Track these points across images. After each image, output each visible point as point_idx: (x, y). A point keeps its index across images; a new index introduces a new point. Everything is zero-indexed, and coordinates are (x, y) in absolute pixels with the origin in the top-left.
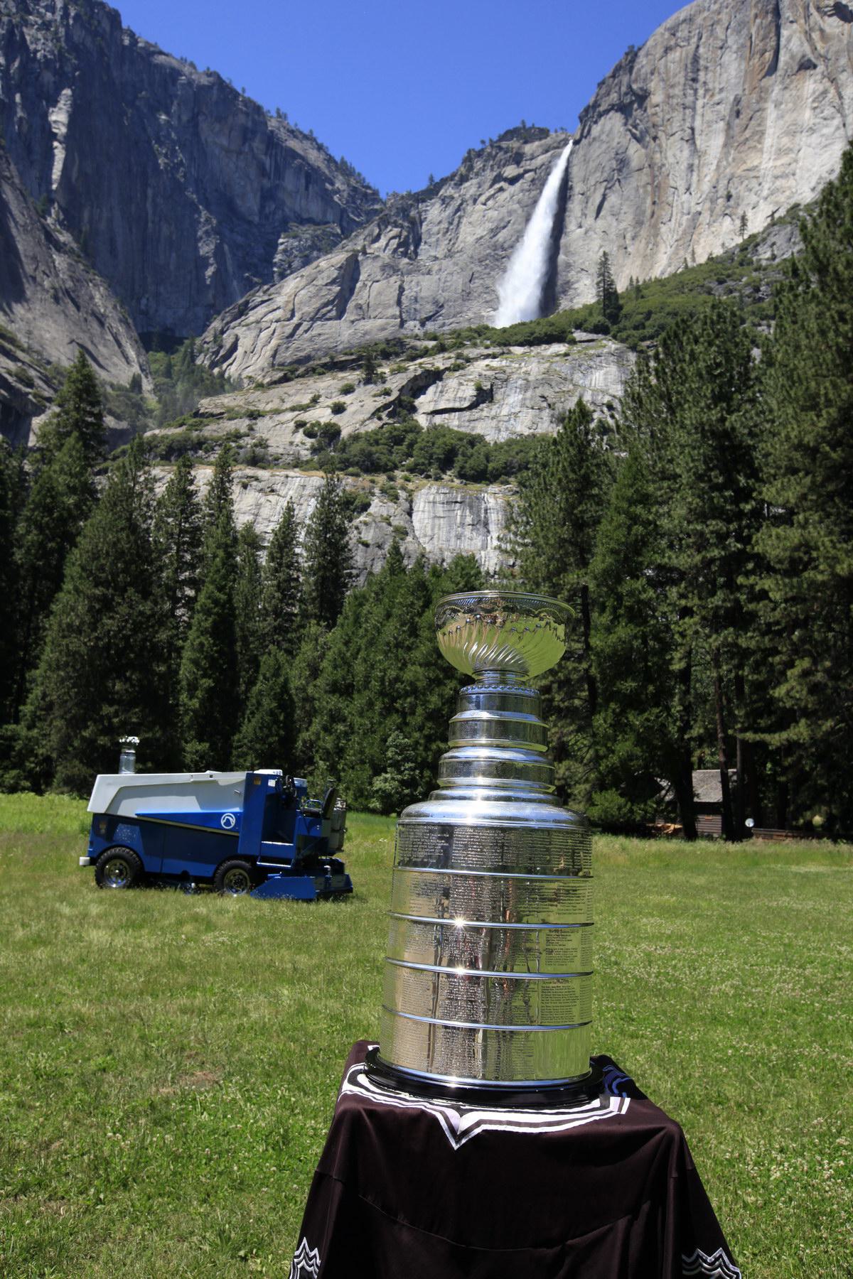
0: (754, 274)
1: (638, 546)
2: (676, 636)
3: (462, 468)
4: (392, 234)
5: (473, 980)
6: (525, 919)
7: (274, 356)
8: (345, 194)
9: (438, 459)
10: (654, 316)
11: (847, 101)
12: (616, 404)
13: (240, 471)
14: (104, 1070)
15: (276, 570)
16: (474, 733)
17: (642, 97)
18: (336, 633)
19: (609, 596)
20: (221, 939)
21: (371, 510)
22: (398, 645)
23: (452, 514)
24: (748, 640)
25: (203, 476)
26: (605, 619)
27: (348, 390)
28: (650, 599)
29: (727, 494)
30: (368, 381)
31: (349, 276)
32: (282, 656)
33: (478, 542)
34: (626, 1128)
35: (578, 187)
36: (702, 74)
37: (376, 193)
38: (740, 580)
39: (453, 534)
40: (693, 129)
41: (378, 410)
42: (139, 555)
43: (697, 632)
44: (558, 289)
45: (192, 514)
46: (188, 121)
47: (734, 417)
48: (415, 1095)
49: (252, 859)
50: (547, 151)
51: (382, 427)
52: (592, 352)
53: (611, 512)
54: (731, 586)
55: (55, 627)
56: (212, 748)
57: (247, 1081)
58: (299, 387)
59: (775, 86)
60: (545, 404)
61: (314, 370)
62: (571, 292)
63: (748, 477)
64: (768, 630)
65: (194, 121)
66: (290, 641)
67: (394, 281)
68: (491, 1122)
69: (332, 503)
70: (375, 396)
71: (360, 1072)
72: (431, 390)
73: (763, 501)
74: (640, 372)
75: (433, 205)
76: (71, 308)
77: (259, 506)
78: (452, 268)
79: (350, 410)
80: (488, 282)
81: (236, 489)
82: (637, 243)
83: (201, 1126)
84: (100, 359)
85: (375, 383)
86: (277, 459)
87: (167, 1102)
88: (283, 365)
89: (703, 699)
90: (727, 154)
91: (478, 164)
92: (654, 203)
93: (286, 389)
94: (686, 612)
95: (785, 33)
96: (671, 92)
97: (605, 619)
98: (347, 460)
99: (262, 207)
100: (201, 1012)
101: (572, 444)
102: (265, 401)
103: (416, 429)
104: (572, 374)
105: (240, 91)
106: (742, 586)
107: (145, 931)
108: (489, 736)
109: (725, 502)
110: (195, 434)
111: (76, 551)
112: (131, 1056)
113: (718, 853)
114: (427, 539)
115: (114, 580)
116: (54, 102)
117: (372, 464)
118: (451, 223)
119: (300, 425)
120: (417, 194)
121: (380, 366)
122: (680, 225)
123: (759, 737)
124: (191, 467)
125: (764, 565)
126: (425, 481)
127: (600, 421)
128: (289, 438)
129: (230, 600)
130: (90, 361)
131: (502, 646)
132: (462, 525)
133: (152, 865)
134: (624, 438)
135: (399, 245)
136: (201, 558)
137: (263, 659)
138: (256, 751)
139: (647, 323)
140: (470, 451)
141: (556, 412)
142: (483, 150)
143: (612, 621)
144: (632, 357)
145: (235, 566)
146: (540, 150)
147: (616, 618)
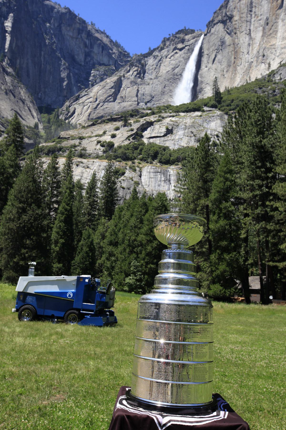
0: (273, 85)
1: (228, 190)
2: (243, 225)
3: (161, 159)
4: (134, 70)
5: (167, 364)
6: (187, 340)
7: (89, 116)
8: (117, 54)
9: (151, 156)
10: (234, 101)
12: (220, 135)
13: (76, 160)
14: (21, 394)
15: (89, 198)
16: (168, 268)
17: (231, 18)
18: (112, 221)
19: (216, 209)
20: (66, 342)
21: (126, 175)
22: (135, 227)
23: (156, 177)
25: (62, 161)
26: (215, 218)
27: (117, 129)
28: (233, 210)
29: (262, 170)
30: (125, 126)
32: (91, 231)
33: (166, 187)
34: (227, 424)
35: (206, 52)
36: (254, 9)
37: (128, 54)
38: (268, 203)
39: (157, 184)
40: (250, 30)
41: (129, 137)
42: (37, 192)
43: (250, 223)
44: (198, 91)
45: (57, 176)
46: (58, 26)
48: (145, 409)
49: (79, 310)
50: (194, 38)
51: (130, 143)
52: (210, 115)
53: (218, 177)
54: (264, 205)
55: (4, 219)
56: (63, 266)
57: (76, 399)
58: (98, 127)
60: (192, 135)
61: (104, 121)
62: (203, 92)
64: (278, 222)
65: (60, 26)
66: (94, 225)
68: (174, 421)
70: (127, 131)
71: (123, 399)
72: (149, 129)
73: (276, 173)
74: (229, 123)
75: (150, 58)
76: (12, 97)
77: (83, 173)
78: (157, 83)
79: (118, 136)
80: (171, 88)
82: (228, 73)
83: (58, 417)
84: (23, 116)
85: (128, 126)
86: (90, 155)
87: (45, 407)
88: (92, 119)
89: (253, 249)
90: (264, 39)
91: (168, 43)
92: (235, 58)
93: (93, 128)
94: (246, 215)
96: (242, 15)
97: (215, 218)
98: (117, 156)
99: (85, 59)
100: (59, 371)
101: (203, 150)
102: (86, 133)
103: (143, 144)
104: (203, 123)
105: (77, 15)
106: (268, 205)
107: (37, 338)
108: (174, 269)
110: (59, 145)
111: (12, 190)
112: (32, 389)
113: (258, 309)
114: (147, 186)
115: (27, 201)
116: (6, 19)
117: (126, 157)
118: (157, 66)
119: (99, 142)
120: (144, 54)
121: (130, 120)
122: (245, 66)
123: (275, 264)
124: (57, 158)
125: (276, 197)
126: (146, 164)
127: (214, 141)
128: (94, 147)
129: (71, 209)
130: (19, 117)
131: (179, 235)
132: (160, 181)
133: (40, 312)
134: (223, 148)
135: (137, 74)
136: (60, 193)
137: (84, 232)
138: (80, 267)
139: (232, 104)
140: (164, 152)
141: (197, 138)
142: (169, 38)
143: (218, 218)
144: (226, 117)
145: (73, 196)
146: (191, 38)
147: (219, 217)
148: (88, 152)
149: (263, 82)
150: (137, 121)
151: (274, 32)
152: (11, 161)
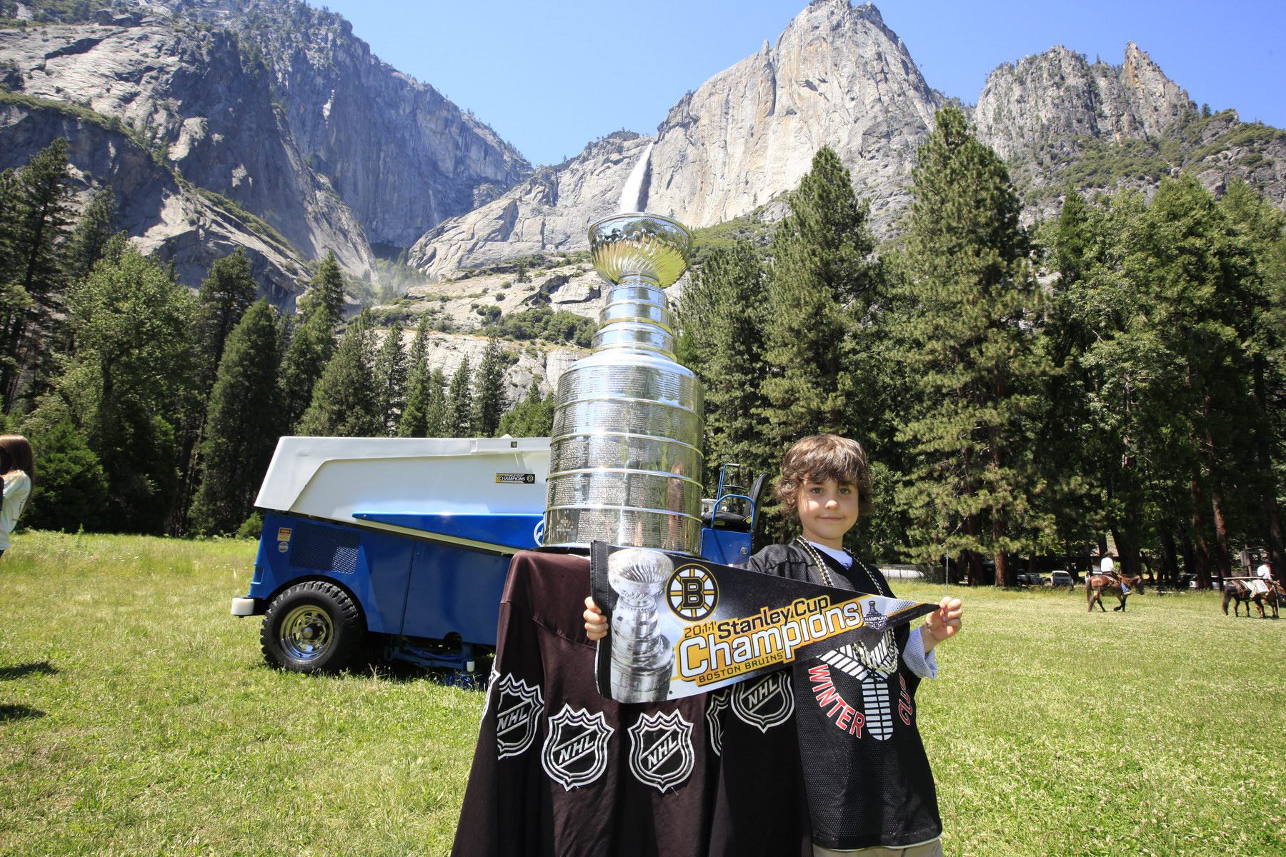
3: (579, 338)
7: (460, 262)
11: (813, 135)
12: (678, 303)
15: (455, 399)
17: (696, 121)
24: (758, 449)
25: (409, 337)
27: (507, 286)
30: (520, 281)
31: (511, 215)
35: (656, 169)
36: (731, 111)
37: (529, 164)
38: (753, 411)
41: (526, 299)
43: (725, 443)
45: (401, 360)
47: (750, 310)
54: (746, 414)
55: (305, 431)
59: (773, 120)
61: (485, 272)
63: (759, 347)
67: (539, 219)
69: (493, 357)
72: (561, 288)
73: (766, 362)
74: (693, 281)
77: (445, 358)
81: (430, 348)
84: (344, 259)
90: (746, 157)
94: (718, 430)
95: (778, 93)
102: (451, 291)
103: (550, 313)
106: (753, 415)
109: (744, 361)
111: (321, 381)
115: (347, 400)
125: (766, 402)
129: (424, 414)
134: (683, 320)
135: (543, 197)
136: (405, 389)
145: (429, 395)
148: (455, 322)
149: (746, 222)
150: (541, 275)
151: (762, 147)
152: (320, 331)
